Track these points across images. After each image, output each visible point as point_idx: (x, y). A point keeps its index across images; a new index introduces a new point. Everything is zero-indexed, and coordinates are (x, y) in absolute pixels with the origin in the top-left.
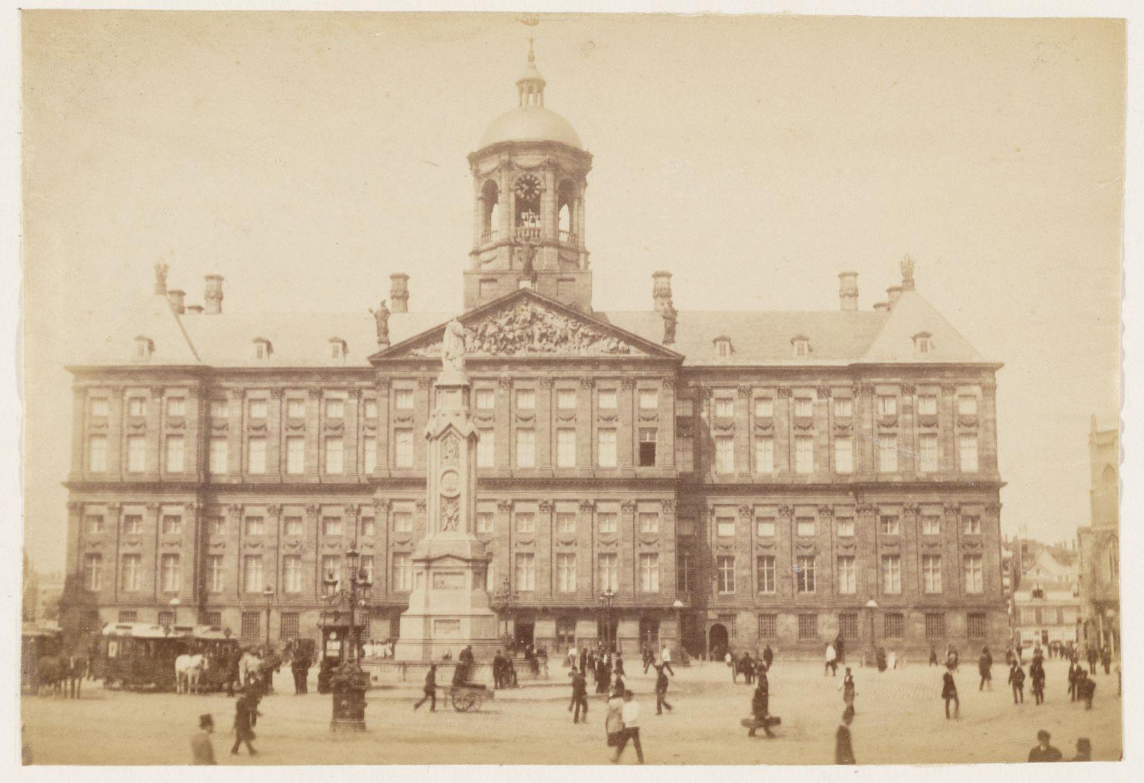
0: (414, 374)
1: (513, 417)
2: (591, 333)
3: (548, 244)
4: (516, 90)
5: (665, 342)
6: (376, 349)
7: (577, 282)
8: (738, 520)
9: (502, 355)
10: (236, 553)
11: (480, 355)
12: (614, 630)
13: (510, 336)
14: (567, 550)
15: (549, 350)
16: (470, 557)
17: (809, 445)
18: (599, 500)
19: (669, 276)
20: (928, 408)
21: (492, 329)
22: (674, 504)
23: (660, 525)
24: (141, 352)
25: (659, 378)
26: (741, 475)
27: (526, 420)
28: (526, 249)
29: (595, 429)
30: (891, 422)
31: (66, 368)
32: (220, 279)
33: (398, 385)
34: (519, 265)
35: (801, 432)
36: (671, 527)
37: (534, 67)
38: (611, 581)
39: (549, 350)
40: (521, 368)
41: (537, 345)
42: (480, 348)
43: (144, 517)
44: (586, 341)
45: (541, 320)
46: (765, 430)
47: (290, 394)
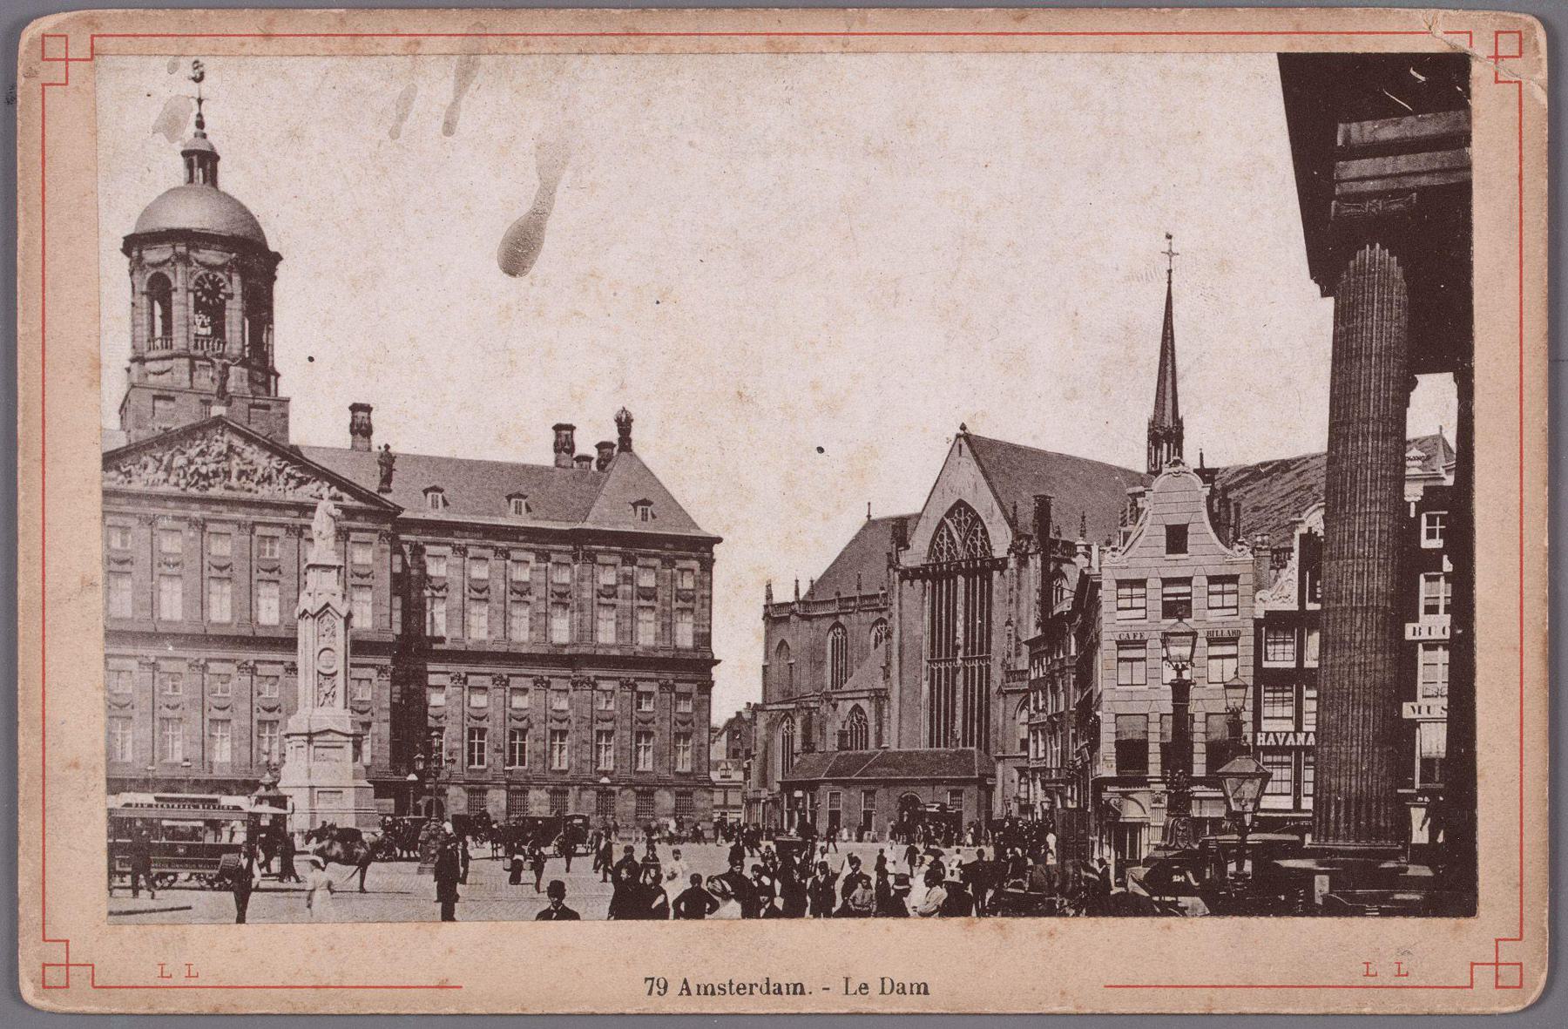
1: (206, 564)
2: (299, 475)
4: (180, 162)
7: (273, 410)
9: (193, 491)
11: (164, 489)
13: (203, 470)
15: (250, 490)
17: (526, 611)
18: (211, 660)
21: (180, 461)
28: (219, 368)
30: (611, 592)
37: (204, 136)
39: (250, 490)
40: (214, 508)
41: (234, 482)
42: (166, 481)
44: (292, 483)
45: (239, 455)
46: (480, 591)
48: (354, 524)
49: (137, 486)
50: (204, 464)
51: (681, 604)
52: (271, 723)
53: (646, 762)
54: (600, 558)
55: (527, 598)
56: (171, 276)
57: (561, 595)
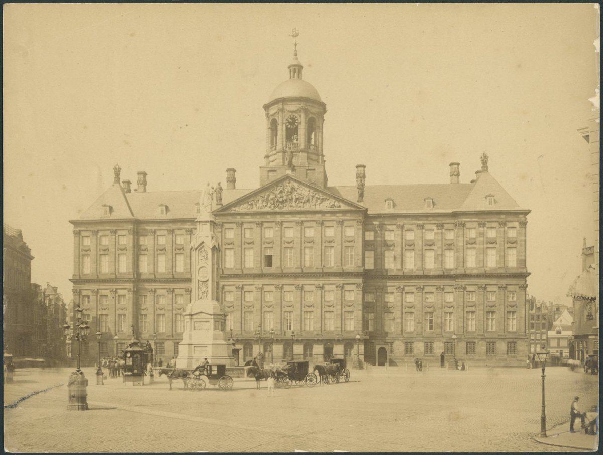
2: (322, 197)
3: (302, 151)
5: (358, 201)
6: (215, 207)
7: (316, 170)
8: (396, 294)
9: (277, 209)
10: (153, 313)
11: (266, 210)
13: (281, 200)
14: (309, 309)
15: (300, 207)
16: (212, 313)
19: (364, 167)
20: (492, 234)
21: (272, 196)
23: (354, 295)
24: (105, 213)
25: (355, 220)
26: (398, 270)
31: (70, 221)
32: (145, 174)
33: (226, 226)
34: (287, 162)
35: (428, 247)
36: (360, 297)
38: (332, 326)
39: (300, 207)
41: (294, 204)
43: (109, 296)
44: (319, 201)
46: (410, 245)
47: (177, 232)
48: (346, 218)
49: (255, 209)
50: (282, 197)
51: (509, 245)
52: (310, 312)
53: (494, 327)
54: (468, 225)
55: (433, 247)
56: (278, 119)
57: (450, 245)
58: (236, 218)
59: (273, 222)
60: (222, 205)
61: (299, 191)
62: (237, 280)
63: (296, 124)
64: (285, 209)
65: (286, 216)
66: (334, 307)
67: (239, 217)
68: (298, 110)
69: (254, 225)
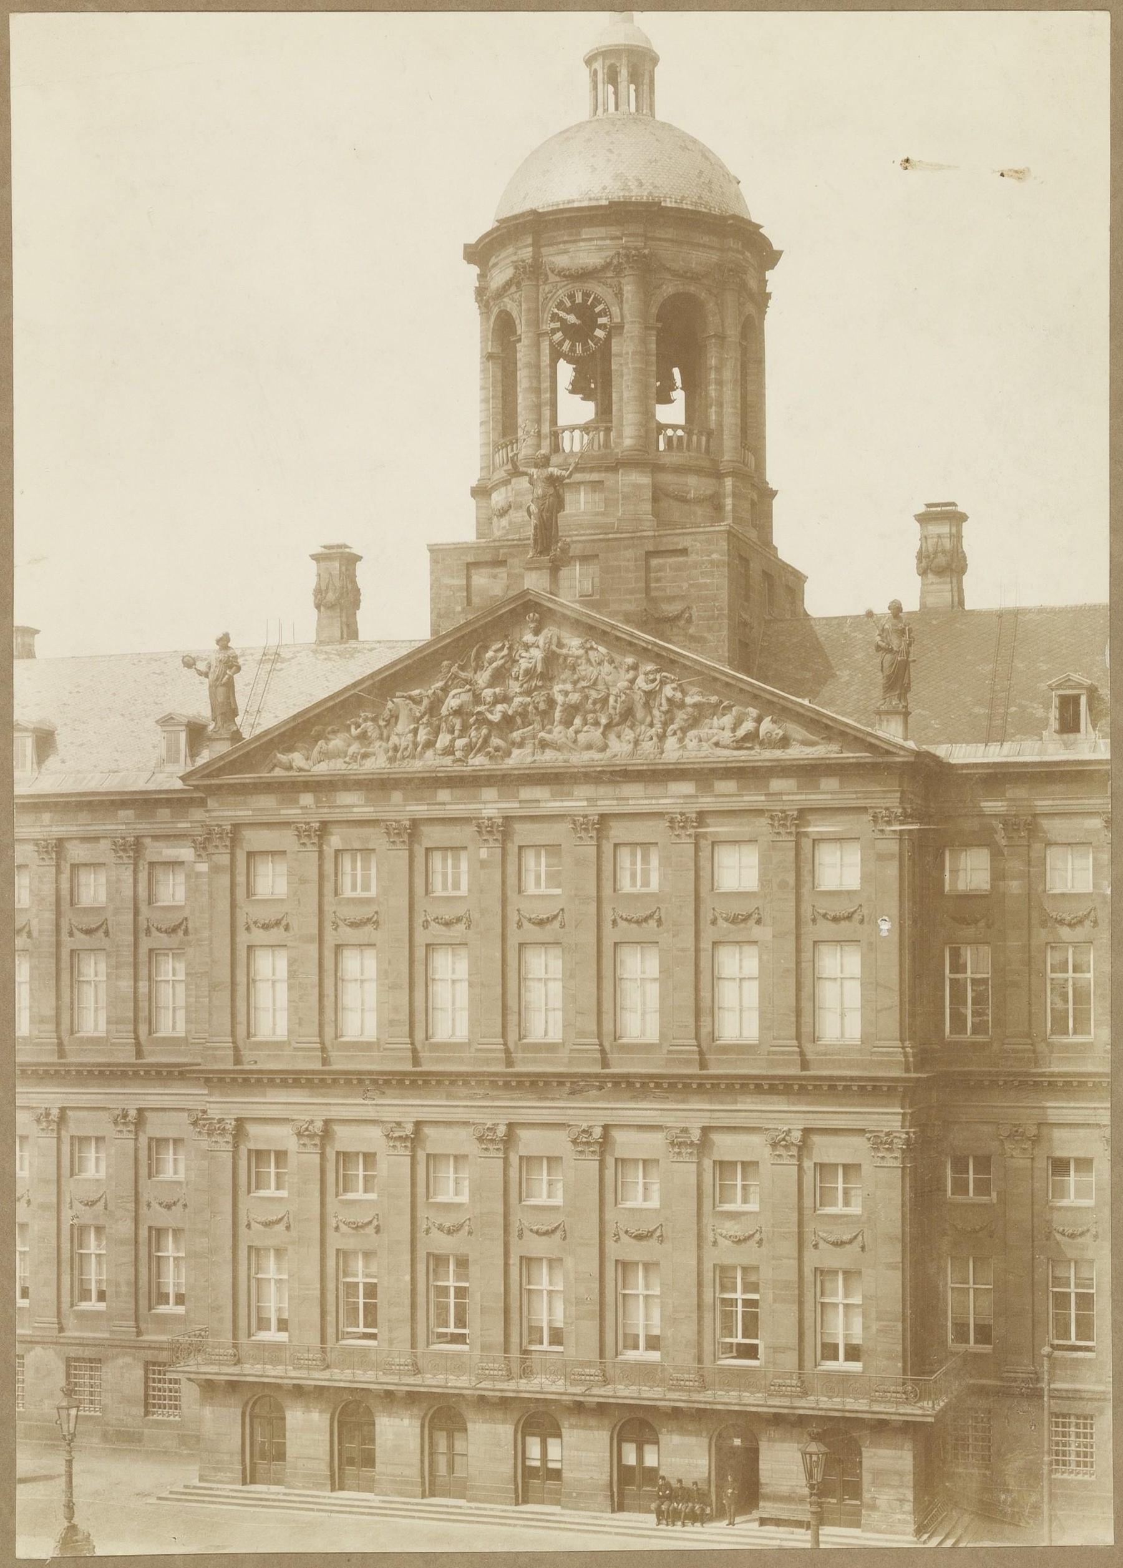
0: (290, 813)
9: (478, 761)
11: (431, 761)
12: (752, 1455)
22: (899, 1144)
27: (541, 923)
29: (706, 945)
33: (255, 839)
39: (589, 747)
41: (557, 733)
42: (430, 744)
50: (506, 699)
56: (515, 314)
58: (297, 801)
59: (466, 820)
60: (236, 736)
61: (584, 669)
62: (299, 1096)
63: (601, 321)
64: (519, 759)
65: (526, 793)
66: (760, 1242)
67: (307, 799)
68: (606, 266)
69: (377, 838)
